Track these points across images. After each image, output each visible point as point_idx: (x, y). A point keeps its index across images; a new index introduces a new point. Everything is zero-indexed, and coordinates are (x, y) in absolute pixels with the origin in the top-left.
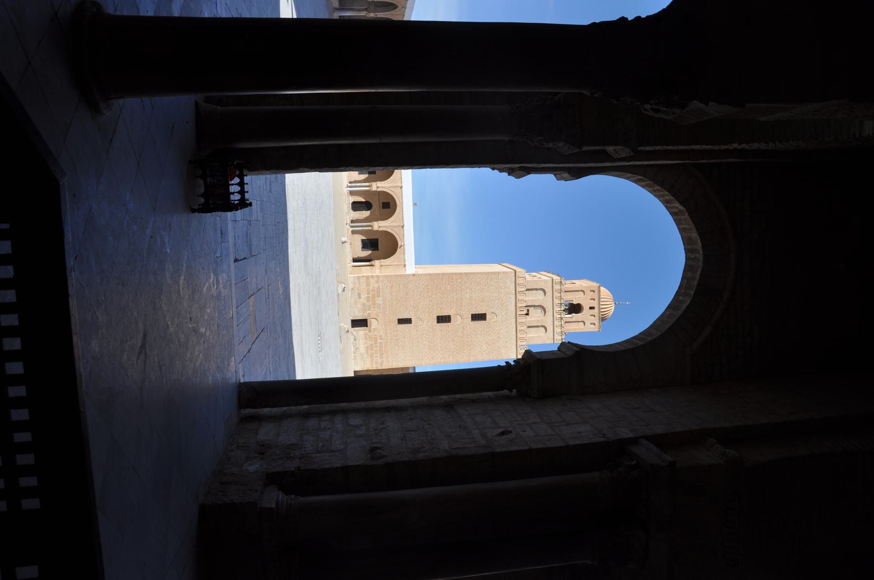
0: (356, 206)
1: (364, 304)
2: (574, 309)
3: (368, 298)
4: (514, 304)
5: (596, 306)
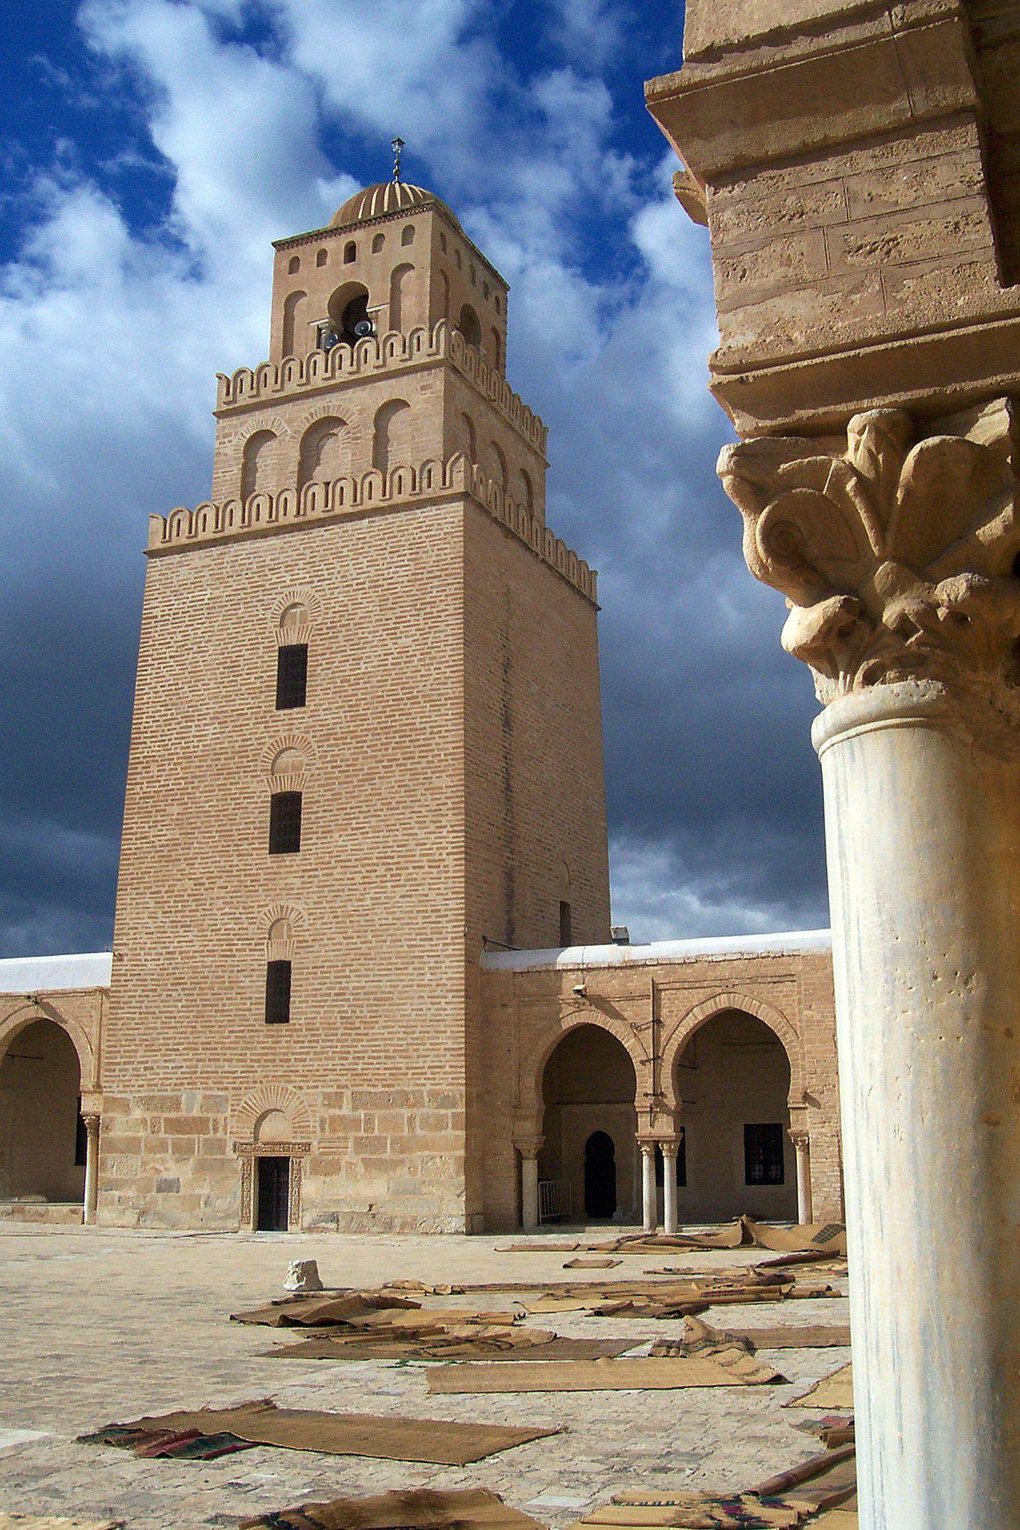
3: (177, 1148)
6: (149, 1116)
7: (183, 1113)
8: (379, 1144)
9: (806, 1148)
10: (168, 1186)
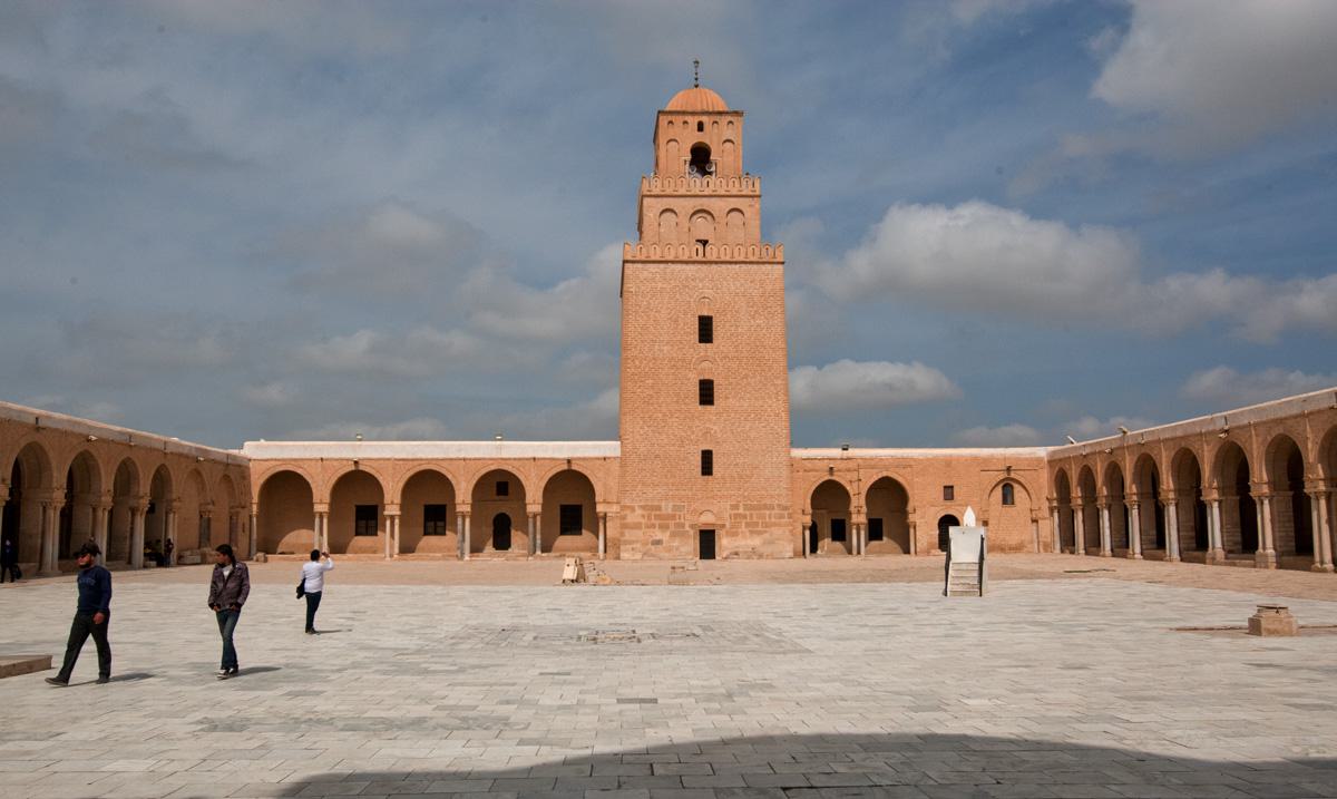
0: (502, 542)
1: (673, 535)
2: (701, 159)
3: (661, 527)
4: (684, 266)
5: (697, 119)
6: (645, 513)
7: (664, 512)
8: (757, 524)
9: (915, 528)
10: (659, 542)
